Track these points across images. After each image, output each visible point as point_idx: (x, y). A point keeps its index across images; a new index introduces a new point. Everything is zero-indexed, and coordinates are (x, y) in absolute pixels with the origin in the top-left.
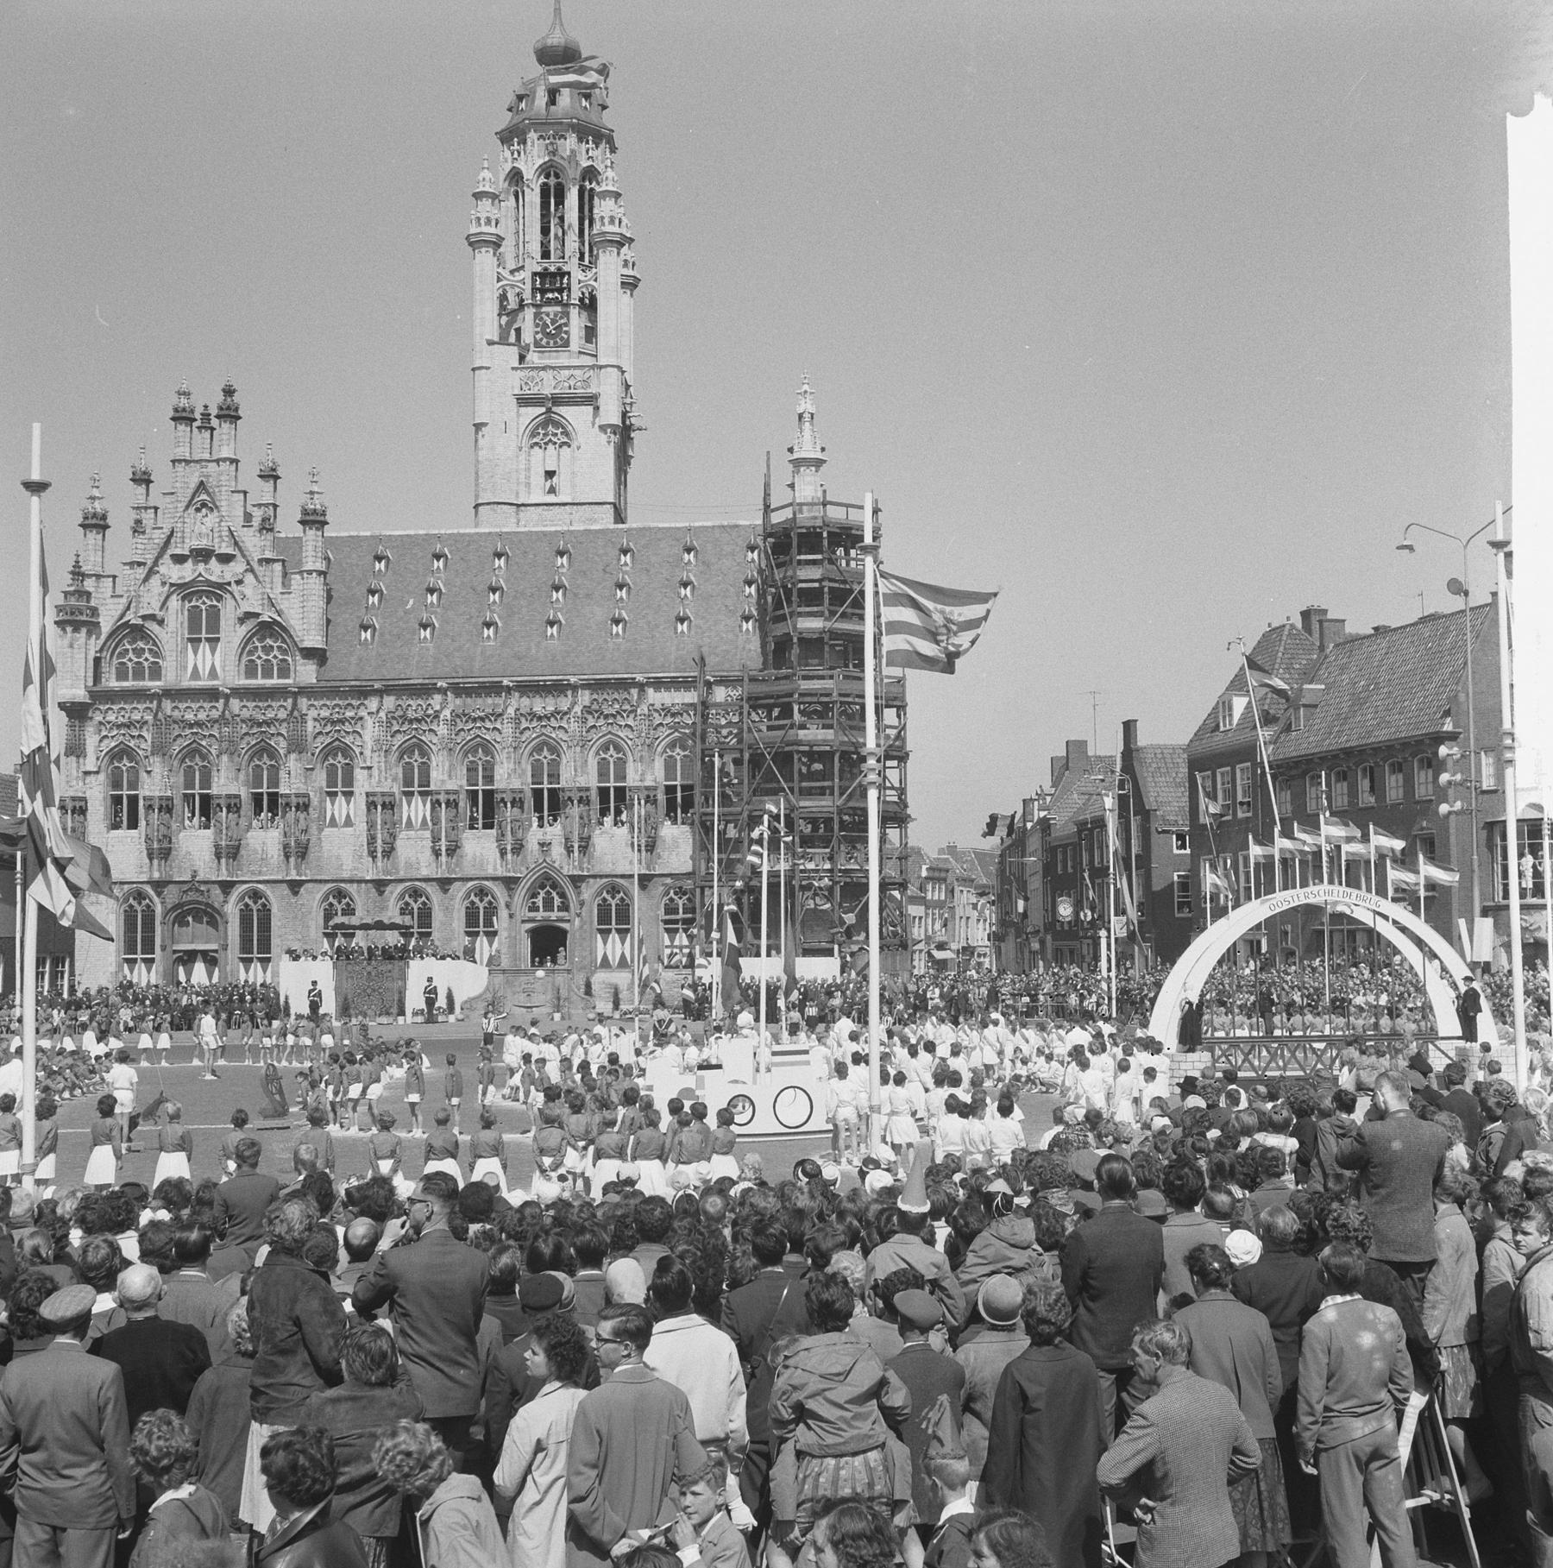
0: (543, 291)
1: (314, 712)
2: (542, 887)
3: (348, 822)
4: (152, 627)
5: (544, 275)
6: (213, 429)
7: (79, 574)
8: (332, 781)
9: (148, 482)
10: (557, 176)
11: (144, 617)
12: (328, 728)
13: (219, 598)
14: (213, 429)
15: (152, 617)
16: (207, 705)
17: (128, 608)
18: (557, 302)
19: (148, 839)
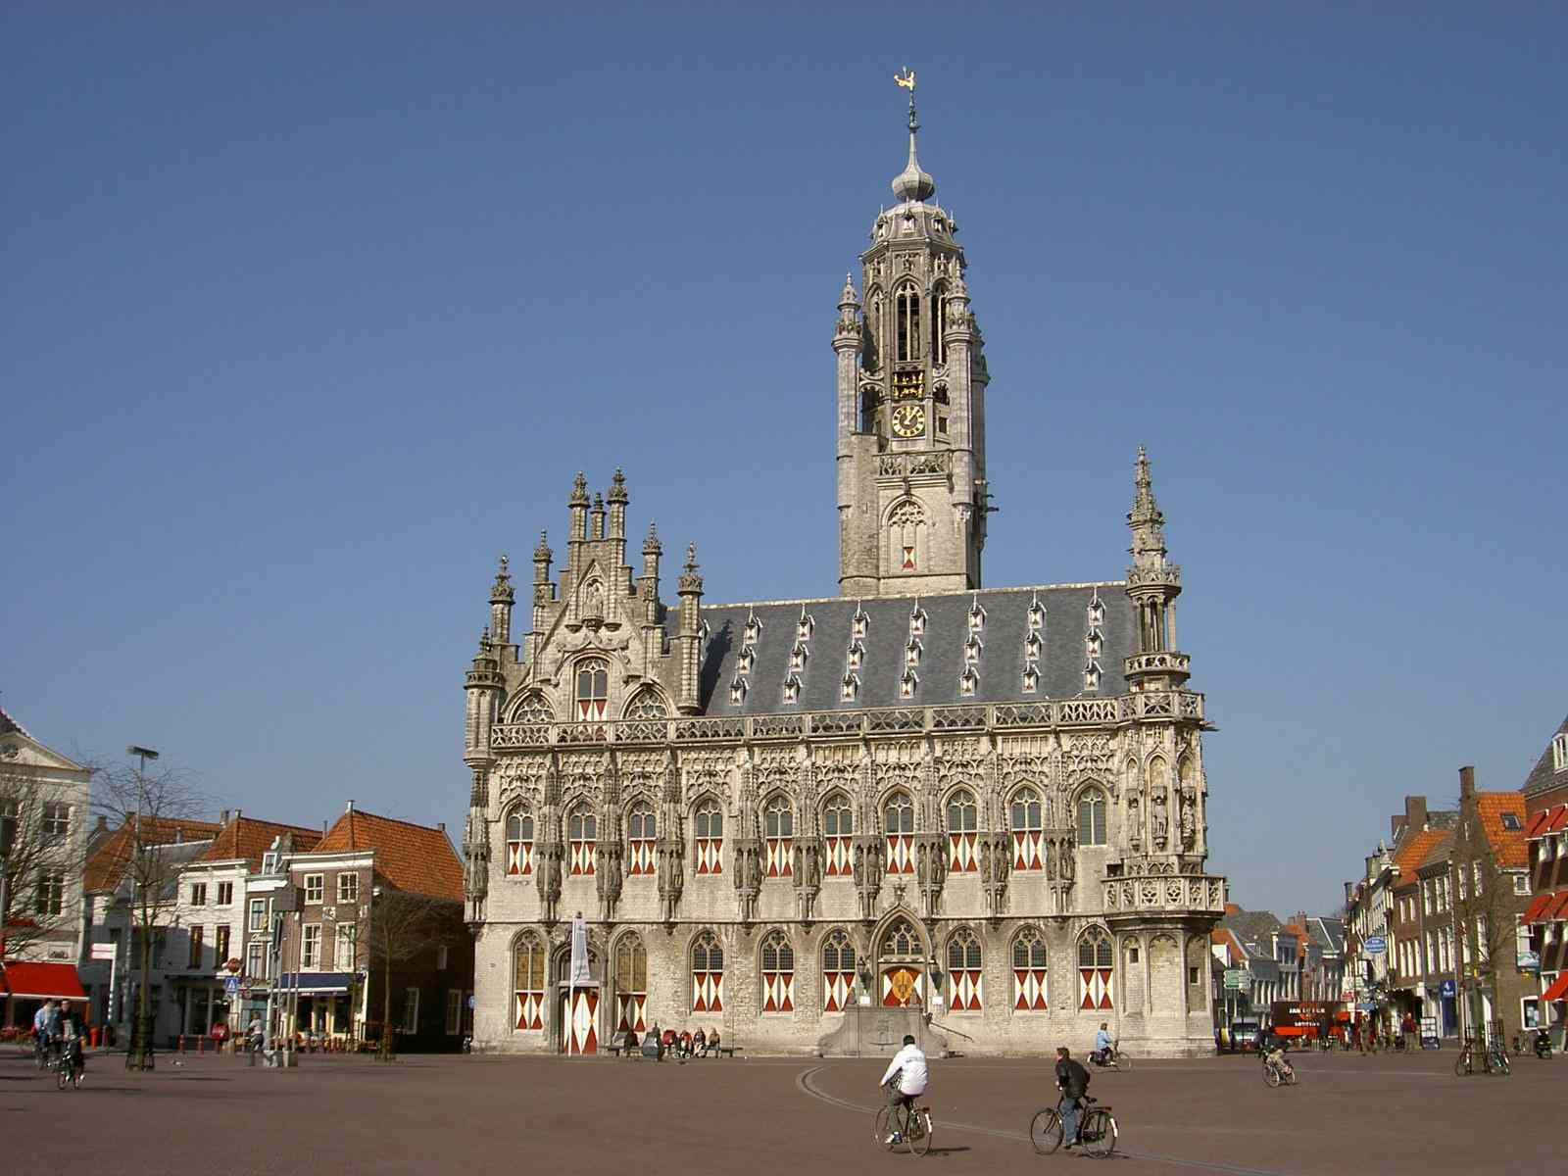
0: (901, 389)
1: (691, 764)
2: (898, 929)
4: (547, 690)
5: (900, 375)
6: (604, 514)
7: (487, 644)
9: (549, 562)
10: (912, 288)
11: (542, 681)
12: (700, 781)
13: (606, 662)
14: (604, 514)
17: (528, 674)
18: (914, 396)
19: (539, 882)
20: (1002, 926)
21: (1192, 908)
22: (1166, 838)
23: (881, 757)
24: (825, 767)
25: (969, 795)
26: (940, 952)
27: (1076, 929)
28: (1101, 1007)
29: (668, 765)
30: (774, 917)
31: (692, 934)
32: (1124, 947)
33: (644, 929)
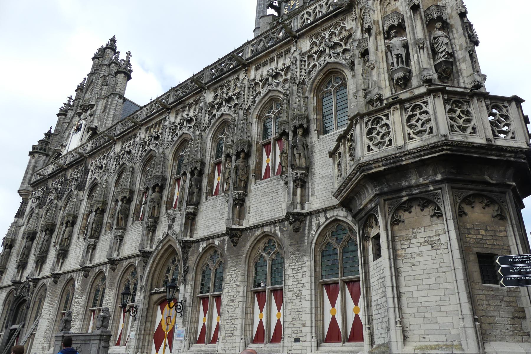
20: (241, 239)
21: (457, 137)
22: (410, 72)
26: (190, 276)
27: (314, 228)
28: (349, 341)
31: (66, 280)
32: (365, 238)
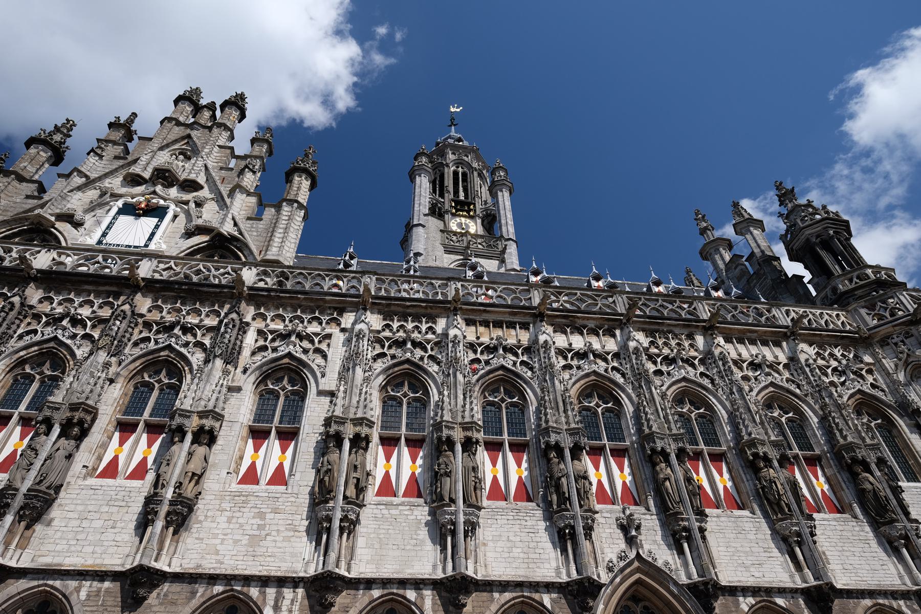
3: (279, 478)
8: (263, 412)
15: (68, 218)
16: (97, 302)
23: (561, 341)
24: (480, 345)
25: (698, 401)
29: (227, 315)
30: (388, 571)
33: (78, 590)
